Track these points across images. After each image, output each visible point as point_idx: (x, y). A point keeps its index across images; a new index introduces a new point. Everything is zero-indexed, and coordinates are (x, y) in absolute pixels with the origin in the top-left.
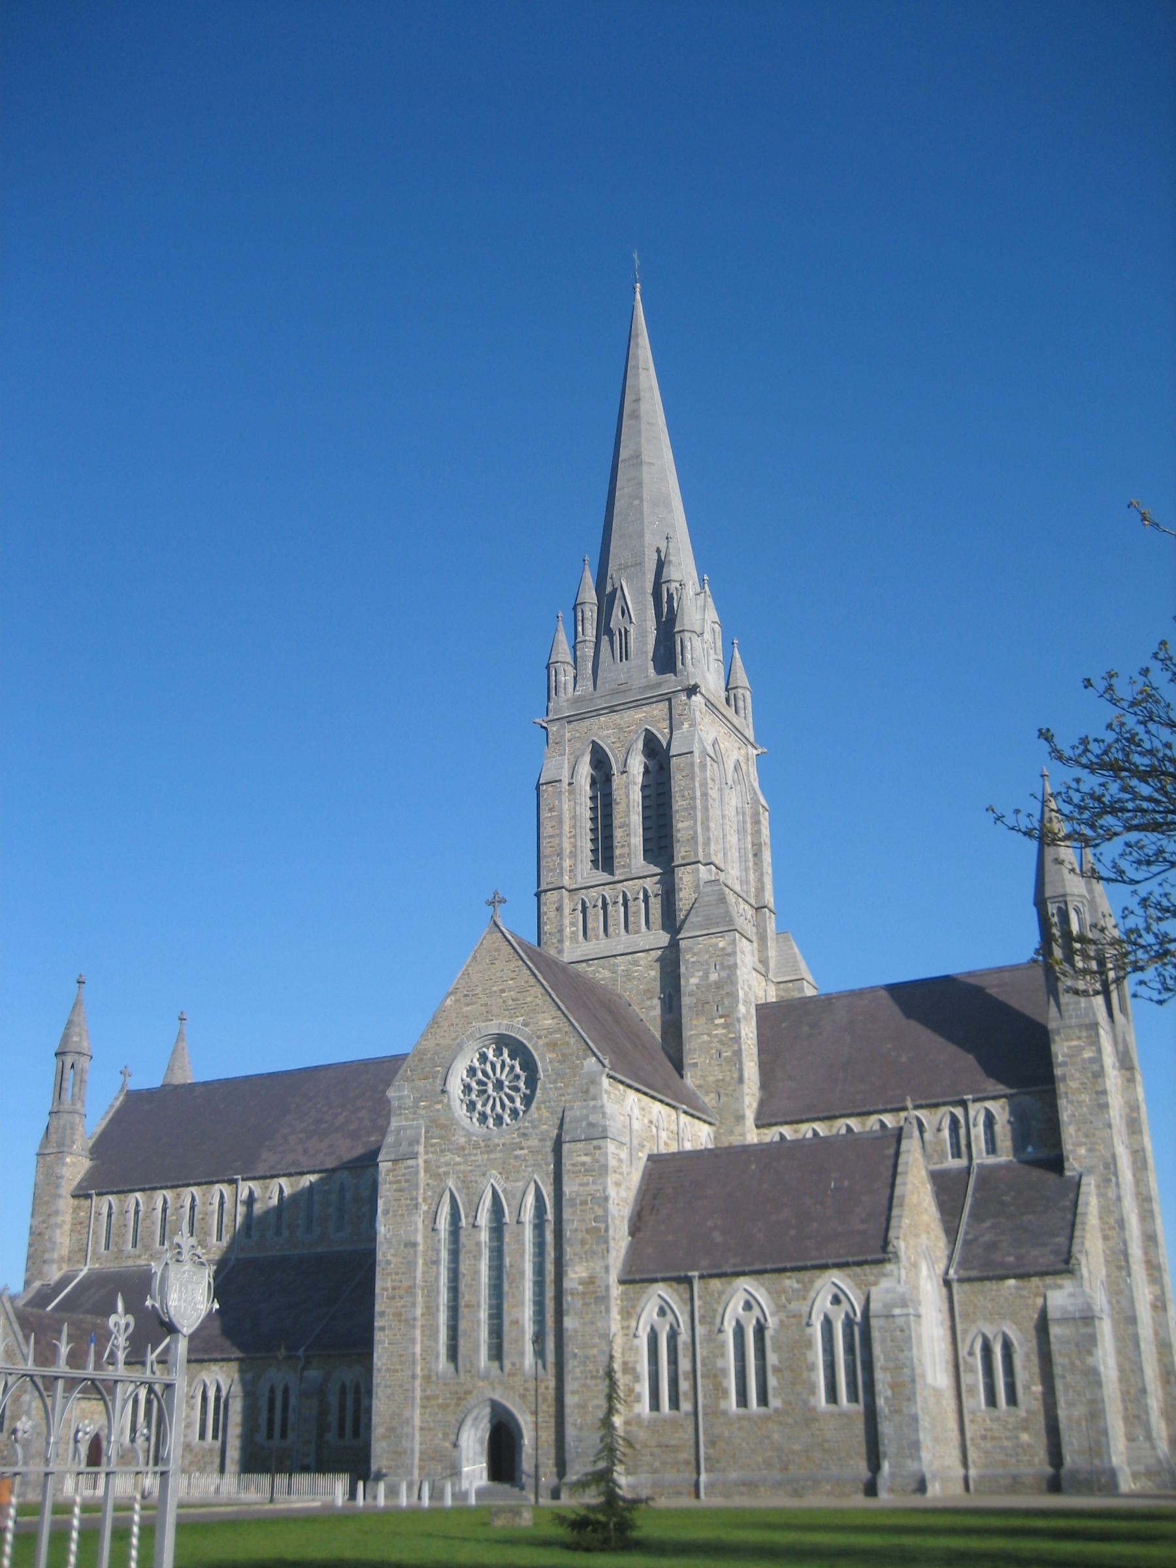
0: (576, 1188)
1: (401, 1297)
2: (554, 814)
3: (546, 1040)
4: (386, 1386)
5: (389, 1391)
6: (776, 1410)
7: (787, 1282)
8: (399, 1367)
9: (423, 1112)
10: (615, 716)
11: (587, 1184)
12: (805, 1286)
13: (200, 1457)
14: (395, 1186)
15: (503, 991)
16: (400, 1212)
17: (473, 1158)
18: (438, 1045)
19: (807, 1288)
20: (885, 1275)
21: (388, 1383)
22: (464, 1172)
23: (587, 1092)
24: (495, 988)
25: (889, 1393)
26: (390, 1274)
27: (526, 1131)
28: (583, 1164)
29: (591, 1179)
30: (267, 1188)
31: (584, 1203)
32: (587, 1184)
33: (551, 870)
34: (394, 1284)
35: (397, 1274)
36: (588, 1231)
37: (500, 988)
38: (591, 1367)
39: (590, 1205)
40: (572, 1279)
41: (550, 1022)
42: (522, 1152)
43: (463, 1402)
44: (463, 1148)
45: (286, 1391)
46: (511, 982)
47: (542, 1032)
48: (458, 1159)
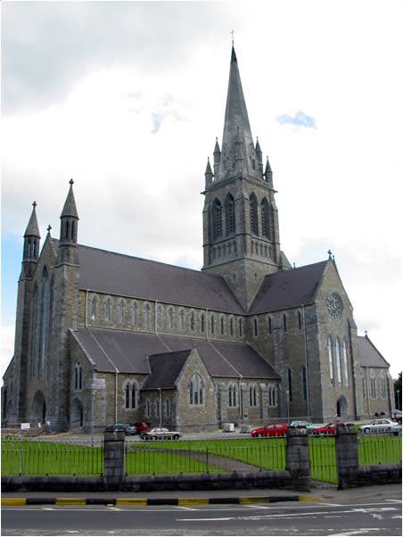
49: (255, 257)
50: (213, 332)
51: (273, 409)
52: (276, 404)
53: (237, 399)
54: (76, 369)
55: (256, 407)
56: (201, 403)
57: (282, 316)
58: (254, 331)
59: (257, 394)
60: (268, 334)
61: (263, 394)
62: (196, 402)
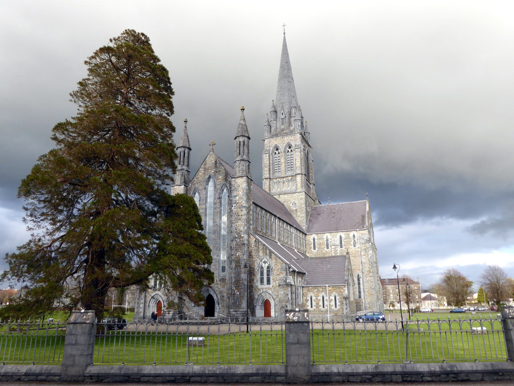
54: (262, 268)
57: (338, 237)
58: (312, 246)
60: (326, 248)
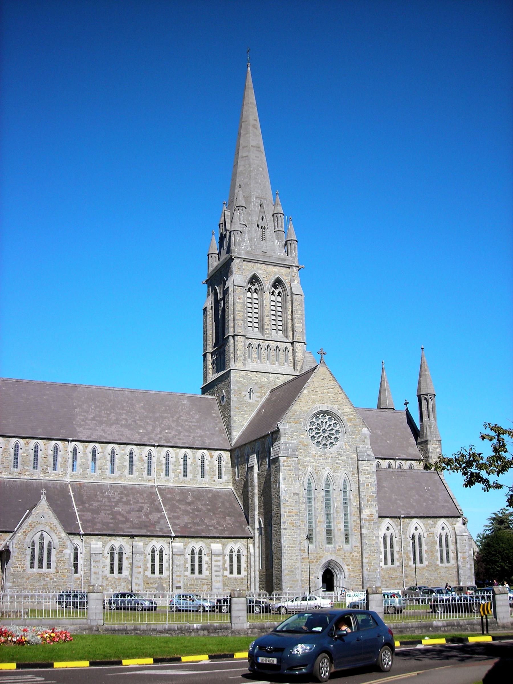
0: (364, 479)
1: (293, 516)
2: (241, 301)
3: (347, 417)
4: (288, 553)
5: (289, 556)
6: (427, 565)
7: (429, 521)
8: (294, 546)
9: (296, 437)
10: (265, 266)
11: (369, 478)
12: (435, 523)
13: (113, 582)
14: (288, 468)
15: (328, 392)
16: (291, 480)
17: (319, 461)
18: (301, 409)
19: (435, 523)
20: (458, 522)
21: (289, 552)
22: (315, 466)
23: (364, 441)
24: (325, 391)
25: (462, 561)
26: (287, 506)
27: (341, 453)
28: (367, 470)
29: (370, 476)
30: (87, 447)
31: (368, 485)
32: (369, 478)
33: (240, 327)
34: (289, 510)
35: (291, 506)
36: (370, 496)
37: (327, 391)
38: (372, 548)
39: (370, 487)
40: (364, 514)
41: (349, 410)
42: (339, 461)
43: (319, 561)
44: (315, 456)
45: (200, 552)
46: (332, 390)
47: (346, 414)
48: (313, 460)
49: (250, 366)
50: (167, 474)
51: (236, 579)
52: (244, 573)
53: (165, 565)
55: (203, 576)
56: (49, 566)
59: (205, 559)
61: (214, 558)
62: (41, 567)
